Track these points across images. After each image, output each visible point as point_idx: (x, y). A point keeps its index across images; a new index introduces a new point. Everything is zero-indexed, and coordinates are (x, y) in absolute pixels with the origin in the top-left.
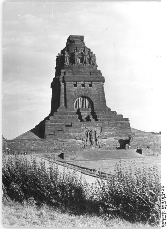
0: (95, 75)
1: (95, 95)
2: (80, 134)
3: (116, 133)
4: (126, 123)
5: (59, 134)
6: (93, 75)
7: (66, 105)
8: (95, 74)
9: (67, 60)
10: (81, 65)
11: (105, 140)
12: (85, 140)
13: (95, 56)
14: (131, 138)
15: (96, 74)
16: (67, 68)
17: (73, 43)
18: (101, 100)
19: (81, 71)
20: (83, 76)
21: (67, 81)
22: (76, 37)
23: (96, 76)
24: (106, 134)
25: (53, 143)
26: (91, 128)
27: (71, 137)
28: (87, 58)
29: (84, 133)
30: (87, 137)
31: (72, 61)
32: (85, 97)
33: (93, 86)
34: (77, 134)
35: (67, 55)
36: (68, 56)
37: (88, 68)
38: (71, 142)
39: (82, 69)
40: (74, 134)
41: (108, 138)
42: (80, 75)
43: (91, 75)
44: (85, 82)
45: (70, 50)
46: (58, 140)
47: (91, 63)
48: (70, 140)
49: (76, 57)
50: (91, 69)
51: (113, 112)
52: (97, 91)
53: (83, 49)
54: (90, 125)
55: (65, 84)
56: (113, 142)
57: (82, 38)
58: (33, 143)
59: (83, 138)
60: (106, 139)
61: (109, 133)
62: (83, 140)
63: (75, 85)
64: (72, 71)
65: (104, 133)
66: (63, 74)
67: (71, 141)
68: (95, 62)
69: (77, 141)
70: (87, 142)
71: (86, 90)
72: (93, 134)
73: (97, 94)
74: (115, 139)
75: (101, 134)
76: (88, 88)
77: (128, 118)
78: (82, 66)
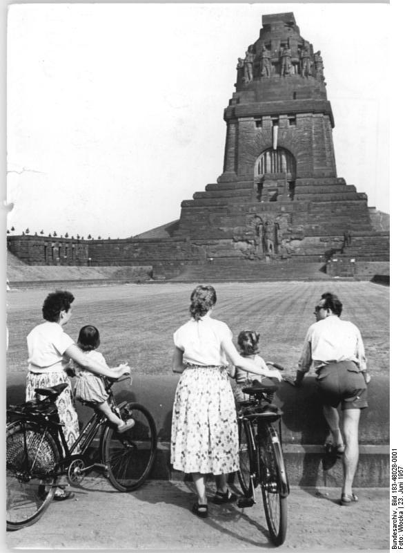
0: (304, 98)
1: (302, 143)
2: (242, 229)
3: (325, 226)
4: (358, 205)
5: (200, 229)
6: (298, 98)
8: (303, 96)
9: (248, 71)
11: (297, 243)
13: (321, 55)
14: (348, 239)
15: (305, 96)
18: (315, 154)
19: (273, 92)
21: (241, 117)
23: (304, 100)
24: (300, 230)
25: (174, 247)
26: (268, 215)
27: (224, 236)
29: (252, 227)
30: (258, 235)
33: (297, 123)
36: (252, 60)
37: (290, 83)
38: (223, 245)
40: (232, 229)
41: (306, 238)
43: (295, 98)
44: (281, 117)
46: (185, 241)
47: (303, 72)
48: (221, 241)
49: (264, 62)
50: (299, 86)
51: (339, 179)
52: (306, 134)
54: (266, 210)
58: (136, 248)
59: (249, 237)
60: (300, 239)
61: (307, 226)
62: (248, 243)
64: (256, 93)
65: (296, 227)
67: (224, 243)
68: (319, 68)
69: (236, 244)
70: (257, 247)
72: (270, 229)
73: (307, 139)
74: (321, 241)
75: (290, 229)
76: (286, 128)
77: (364, 194)
78: (276, 81)
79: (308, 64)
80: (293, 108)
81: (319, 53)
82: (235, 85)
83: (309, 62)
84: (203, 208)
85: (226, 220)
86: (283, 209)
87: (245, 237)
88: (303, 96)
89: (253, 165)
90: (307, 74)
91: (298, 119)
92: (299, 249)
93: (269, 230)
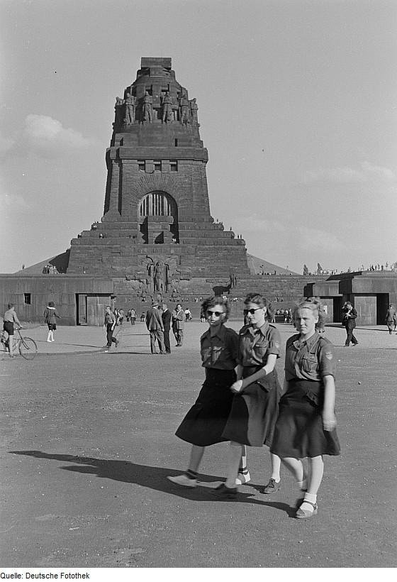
2: (134, 268)
7: (120, 210)
8: (184, 143)
10: (158, 124)
12: (145, 280)
13: (196, 103)
15: (187, 143)
16: (129, 131)
17: (148, 76)
18: (194, 200)
20: (158, 148)
22: (154, 61)
28: (170, 110)
30: (149, 275)
31: (140, 116)
32: (161, 193)
33: (179, 169)
34: (128, 269)
35: (132, 101)
37: (171, 130)
39: (157, 133)
42: (153, 145)
43: (176, 145)
45: (138, 89)
47: (182, 119)
50: (179, 133)
53: (167, 89)
55: (121, 166)
56: (204, 288)
57: (166, 64)
59: (141, 277)
61: (195, 268)
63: (143, 166)
64: (138, 136)
66: (119, 143)
68: (194, 116)
70: (149, 285)
71: (164, 176)
72: (161, 270)
73: (188, 186)
79: (186, 112)
80: (174, 155)
81: (194, 100)
82: (113, 124)
83: (186, 110)
84: (93, 246)
85: (117, 259)
86: (172, 252)
87: (137, 277)
88: (184, 143)
89: (137, 207)
90: (186, 121)
91: (179, 165)
92: (187, 289)
93: (160, 270)
